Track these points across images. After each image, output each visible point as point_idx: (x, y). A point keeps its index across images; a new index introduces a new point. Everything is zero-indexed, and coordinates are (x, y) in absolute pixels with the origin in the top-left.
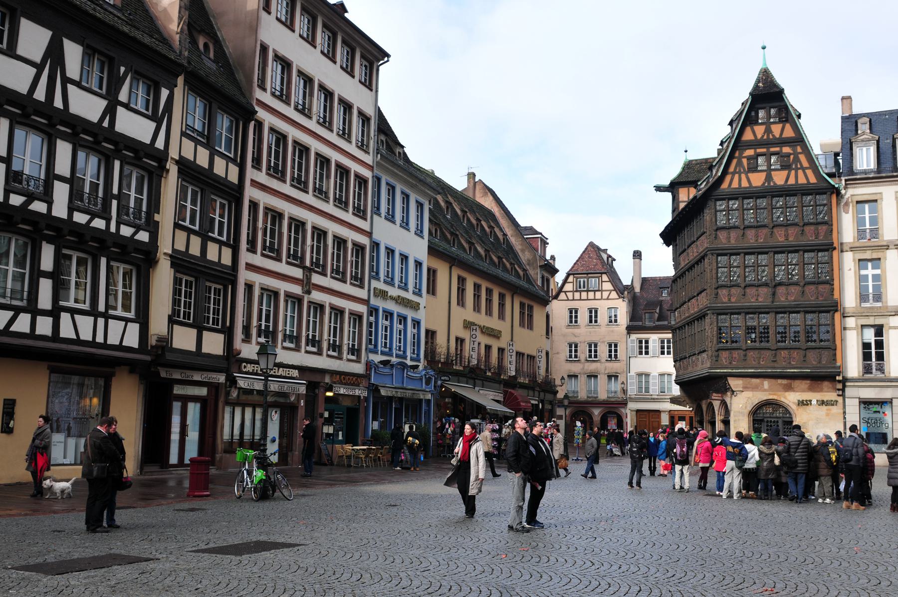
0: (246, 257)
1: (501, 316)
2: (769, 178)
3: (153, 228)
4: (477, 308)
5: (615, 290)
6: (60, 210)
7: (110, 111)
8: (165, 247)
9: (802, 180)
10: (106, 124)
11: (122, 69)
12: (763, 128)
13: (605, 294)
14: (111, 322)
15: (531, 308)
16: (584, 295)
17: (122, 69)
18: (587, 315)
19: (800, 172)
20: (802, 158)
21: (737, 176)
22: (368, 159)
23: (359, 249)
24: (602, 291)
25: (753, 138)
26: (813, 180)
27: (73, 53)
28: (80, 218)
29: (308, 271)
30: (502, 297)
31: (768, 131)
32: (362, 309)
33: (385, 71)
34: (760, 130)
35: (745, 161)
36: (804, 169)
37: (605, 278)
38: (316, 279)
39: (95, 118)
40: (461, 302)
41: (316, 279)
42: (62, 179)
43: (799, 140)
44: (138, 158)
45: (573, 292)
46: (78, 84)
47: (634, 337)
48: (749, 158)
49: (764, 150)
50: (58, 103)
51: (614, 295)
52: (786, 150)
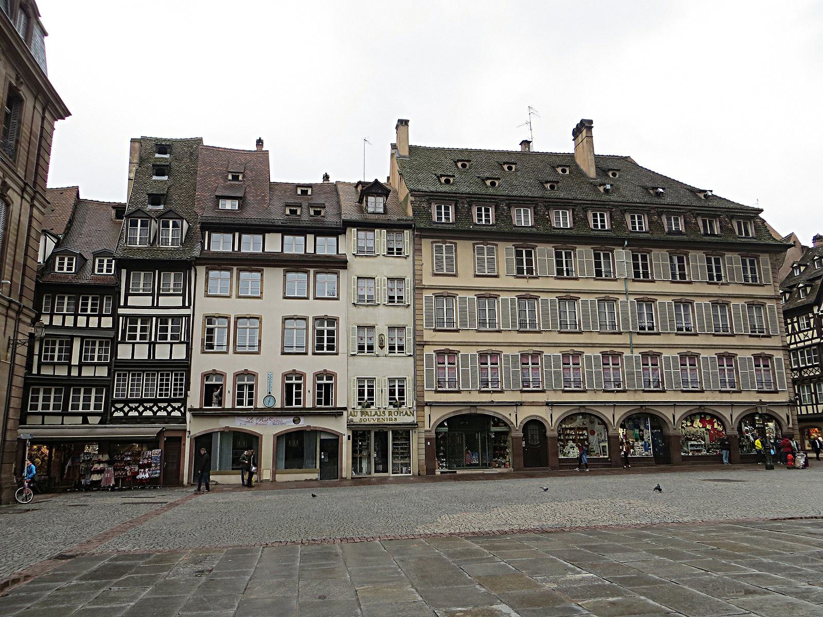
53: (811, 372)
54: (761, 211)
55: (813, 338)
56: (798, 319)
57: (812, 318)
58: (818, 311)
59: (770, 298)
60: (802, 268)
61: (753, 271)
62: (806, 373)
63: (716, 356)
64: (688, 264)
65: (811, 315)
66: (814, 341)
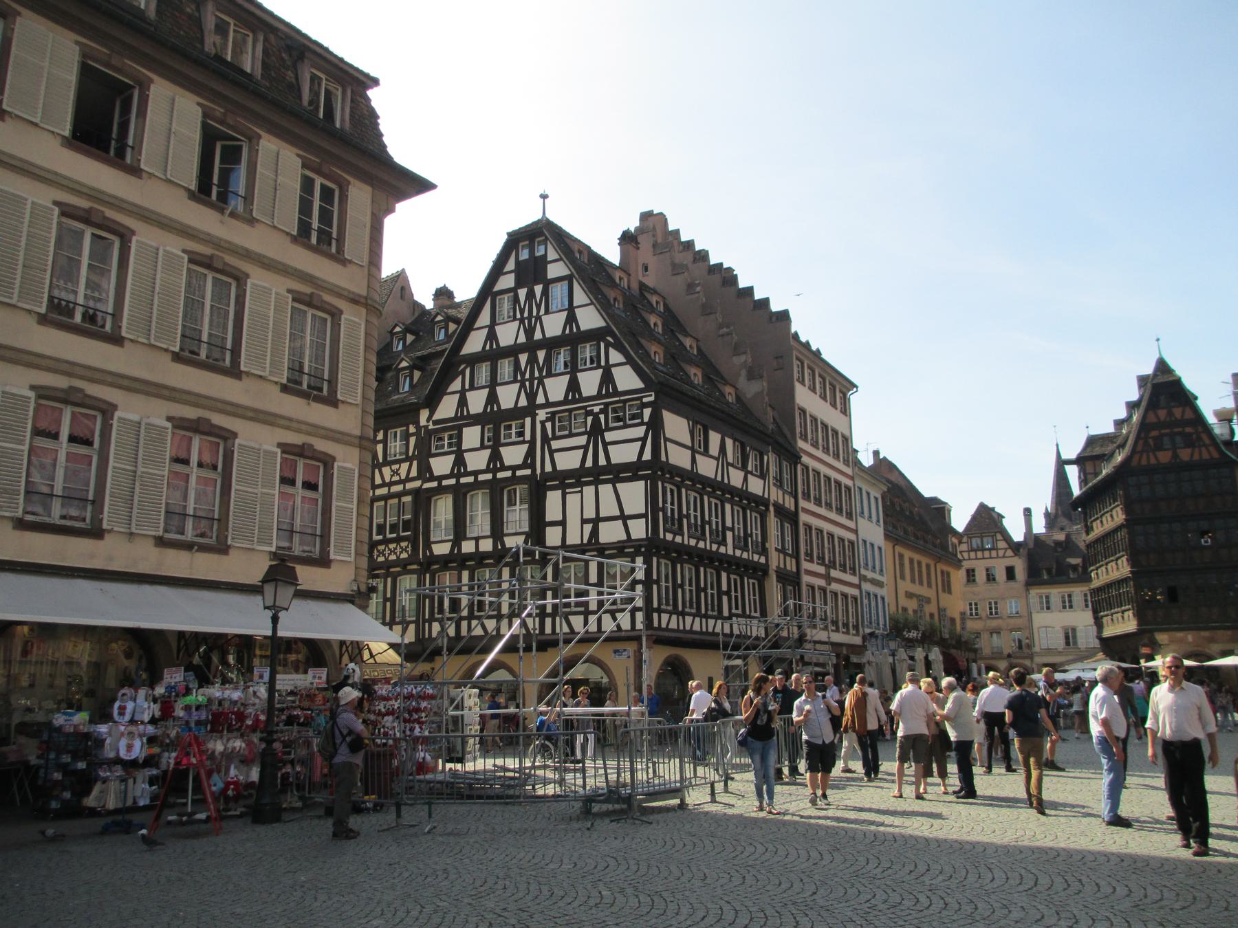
0: (806, 565)
1: (929, 585)
2: (1175, 456)
3: (764, 551)
4: (913, 581)
5: (1010, 548)
6: (730, 552)
7: (745, 479)
8: (773, 564)
9: (1206, 456)
12: (1165, 411)
13: (1001, 553)
15: (948, 574)
16: (979, 554)
18: (984, 573)
19: (1203, 449)
20: (1204, 436)
21: (1145, 456)
22: (849, 471)
23: (851, 543)
24: (997, 549)
25: (1155, 420)
26: (1216, 455)
28: (738, 553)
29: (828, 567)
30: (928, 566)
31: (1170, 414)
32: (856, 592)
33: (855, 400)
34: (1162, 414)
35: (1151, 442)
36: (1205, 445)
37: (999, 537)
38: (834, 573)
40: (903, 577)
41: (834, 573)
42: (729, 529)
43: (1199, 419)
44: (757, 506)
45: (969, 551)
46: (732, 465)
47: (1034, 592)
48: (1155, 438)
49: (1167, 431)
51: (1010, 553)
52: (1188, 430)
53: (392, 552)
54: (375, 82)
55: (408, 479)
56: (385, 435)
57: (413, 435)
58: (428, 421)
59: (355, 300)
60: (410, 338)
61: (325, 217)
62: (382, 553)
63: (169, 425)
64: (142, 113)
65: (412, 429)
66: (409, 486)
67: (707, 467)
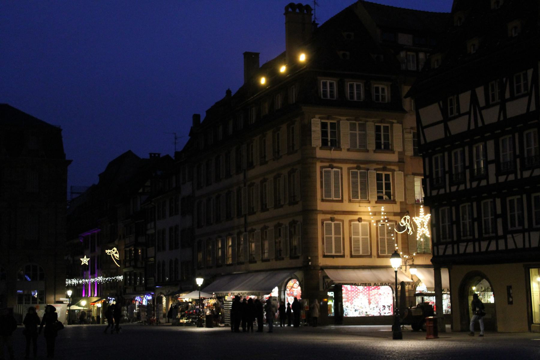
6: (492, 180)
10: (502, 119)
11: (504, 79)
14: (531, 233)
17: (504, 79)
27: (480, 92)
39: (495, 120)
50: (480, 124)
67: (458, 126)
